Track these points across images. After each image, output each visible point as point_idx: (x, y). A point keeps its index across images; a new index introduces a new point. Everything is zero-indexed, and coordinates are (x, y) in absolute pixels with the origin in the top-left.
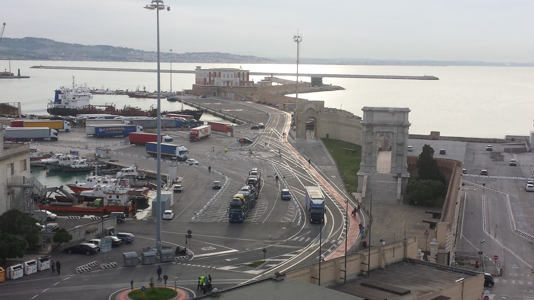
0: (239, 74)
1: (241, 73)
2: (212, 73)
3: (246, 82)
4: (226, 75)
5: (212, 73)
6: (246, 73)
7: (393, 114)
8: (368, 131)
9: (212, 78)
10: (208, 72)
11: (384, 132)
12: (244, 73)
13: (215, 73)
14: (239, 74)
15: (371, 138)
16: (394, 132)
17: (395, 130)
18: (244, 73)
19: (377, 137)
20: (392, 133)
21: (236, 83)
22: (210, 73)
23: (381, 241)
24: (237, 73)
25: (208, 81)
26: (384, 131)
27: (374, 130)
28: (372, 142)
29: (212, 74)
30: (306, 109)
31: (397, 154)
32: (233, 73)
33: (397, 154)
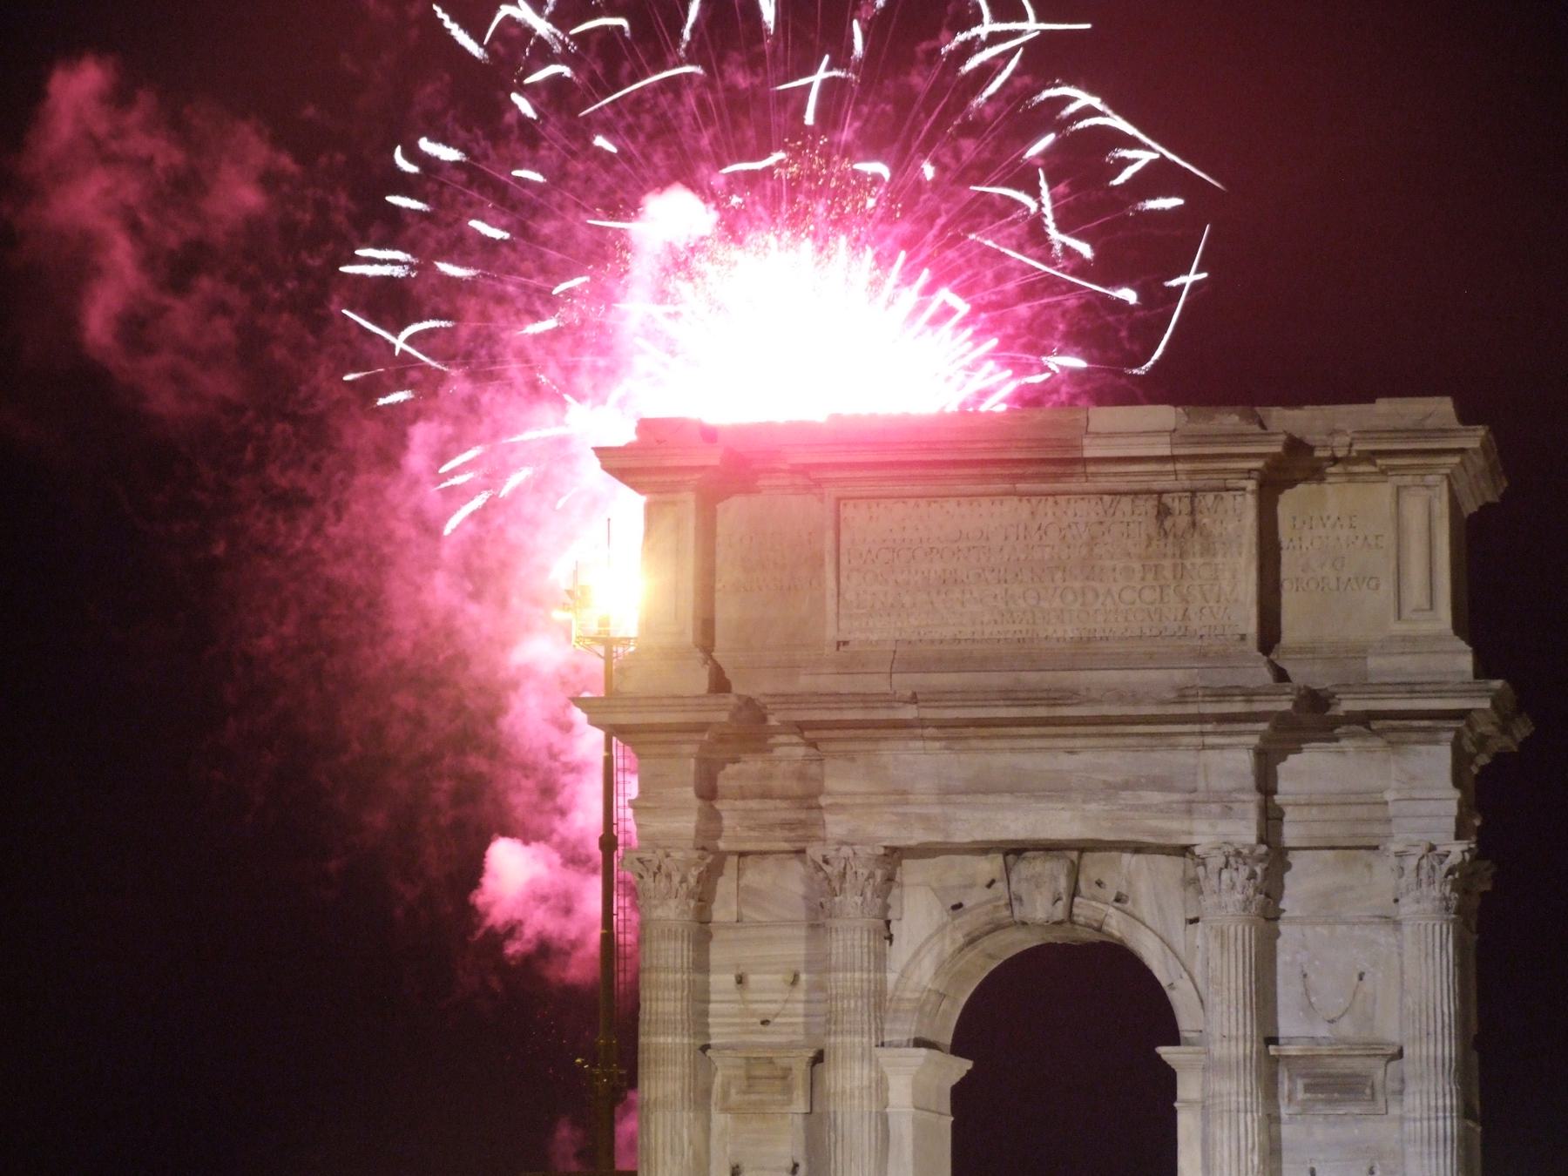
7: (1163, 512)
8: (742, 854)
11: (1015, 851)
15: (795, 981)
16: (1204, 834)
19: (900, 953)
26: (1016, 825)
27: (836, 826)
28: (819, 1058)
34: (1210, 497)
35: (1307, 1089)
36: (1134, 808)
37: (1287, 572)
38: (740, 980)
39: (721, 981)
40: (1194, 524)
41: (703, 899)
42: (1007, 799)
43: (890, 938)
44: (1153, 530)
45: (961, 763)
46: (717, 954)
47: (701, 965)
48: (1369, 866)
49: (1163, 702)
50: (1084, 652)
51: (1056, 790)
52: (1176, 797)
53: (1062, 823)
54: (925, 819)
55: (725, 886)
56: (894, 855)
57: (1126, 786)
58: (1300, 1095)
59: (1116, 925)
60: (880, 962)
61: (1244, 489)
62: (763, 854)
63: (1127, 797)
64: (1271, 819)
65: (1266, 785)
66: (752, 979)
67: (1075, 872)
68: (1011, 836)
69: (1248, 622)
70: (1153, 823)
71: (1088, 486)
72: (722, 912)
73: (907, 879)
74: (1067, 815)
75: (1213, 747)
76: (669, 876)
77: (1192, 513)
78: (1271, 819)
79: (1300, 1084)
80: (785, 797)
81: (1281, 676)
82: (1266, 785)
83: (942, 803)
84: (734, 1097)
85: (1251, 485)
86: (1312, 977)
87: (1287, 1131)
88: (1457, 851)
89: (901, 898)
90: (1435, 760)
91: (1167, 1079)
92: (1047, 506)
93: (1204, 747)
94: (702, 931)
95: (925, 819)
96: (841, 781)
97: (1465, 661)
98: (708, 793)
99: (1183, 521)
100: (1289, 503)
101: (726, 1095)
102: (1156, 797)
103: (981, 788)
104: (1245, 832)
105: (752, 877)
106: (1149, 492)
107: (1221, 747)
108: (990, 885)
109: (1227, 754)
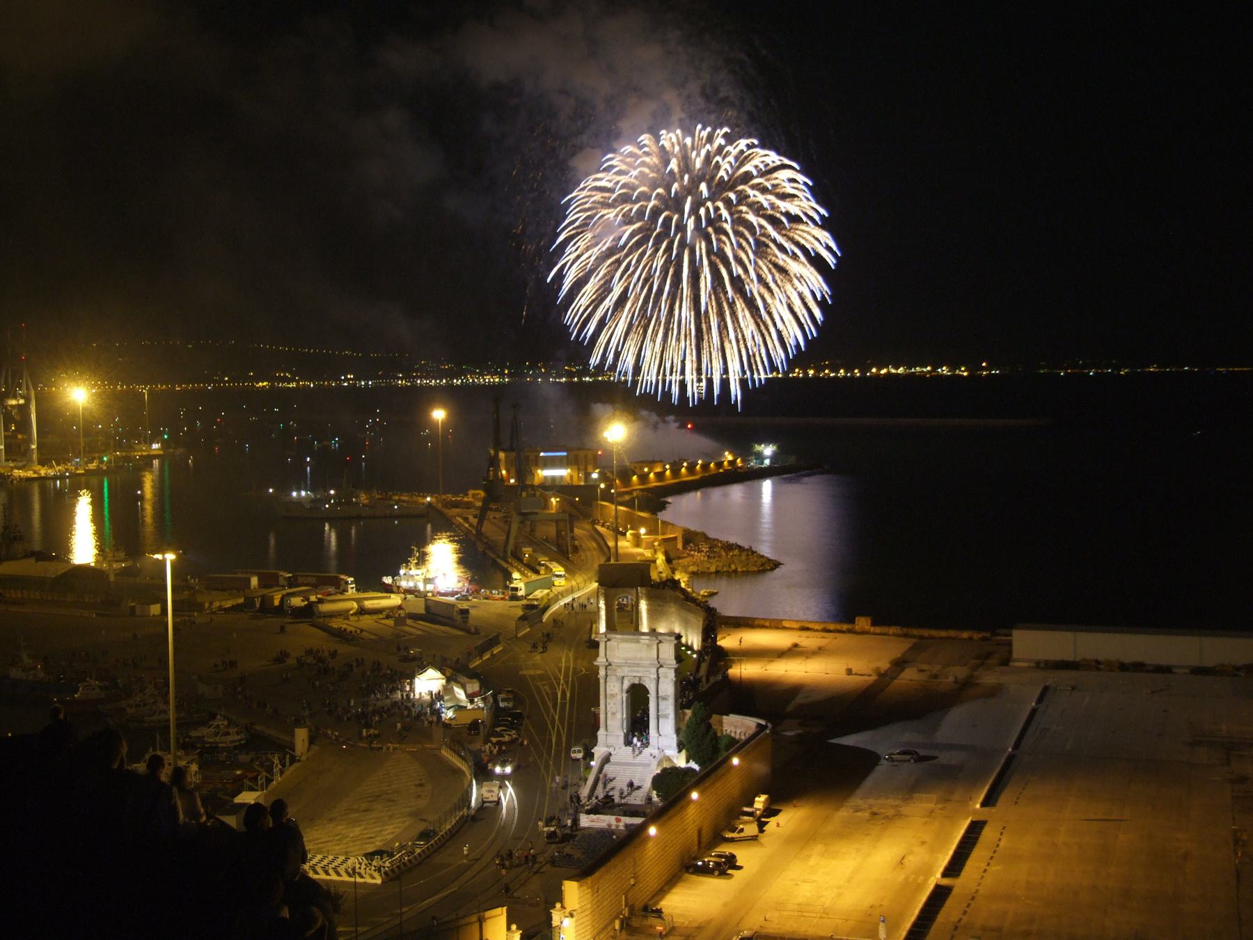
7: (648, 646)
23: (434, 918)
37: (660, 651)
39: (607, 687)
41: (606, 679)
45: (630, 669)
46: (608, 684)
47: (606, 686)
50: (641, 659)
51: (638, 672)
56: (623, 677)
59: (644, 684)
60: (622, 686)
64: (658, 674)
65: (657, 671)
69: (656, 657)
78: (658, 674)
81: (659, 662)
82: (657, 671)
87: (660, 703)
88: (674, 679)
90: (673, 671)
91: (648, 698)
94: (606, 682)
96: (619, 670)
97: (674, 662)
98: (606, 669)
100: (660, 645)
103: (631, 671)
104: (655, 676)
105: (611, 677)
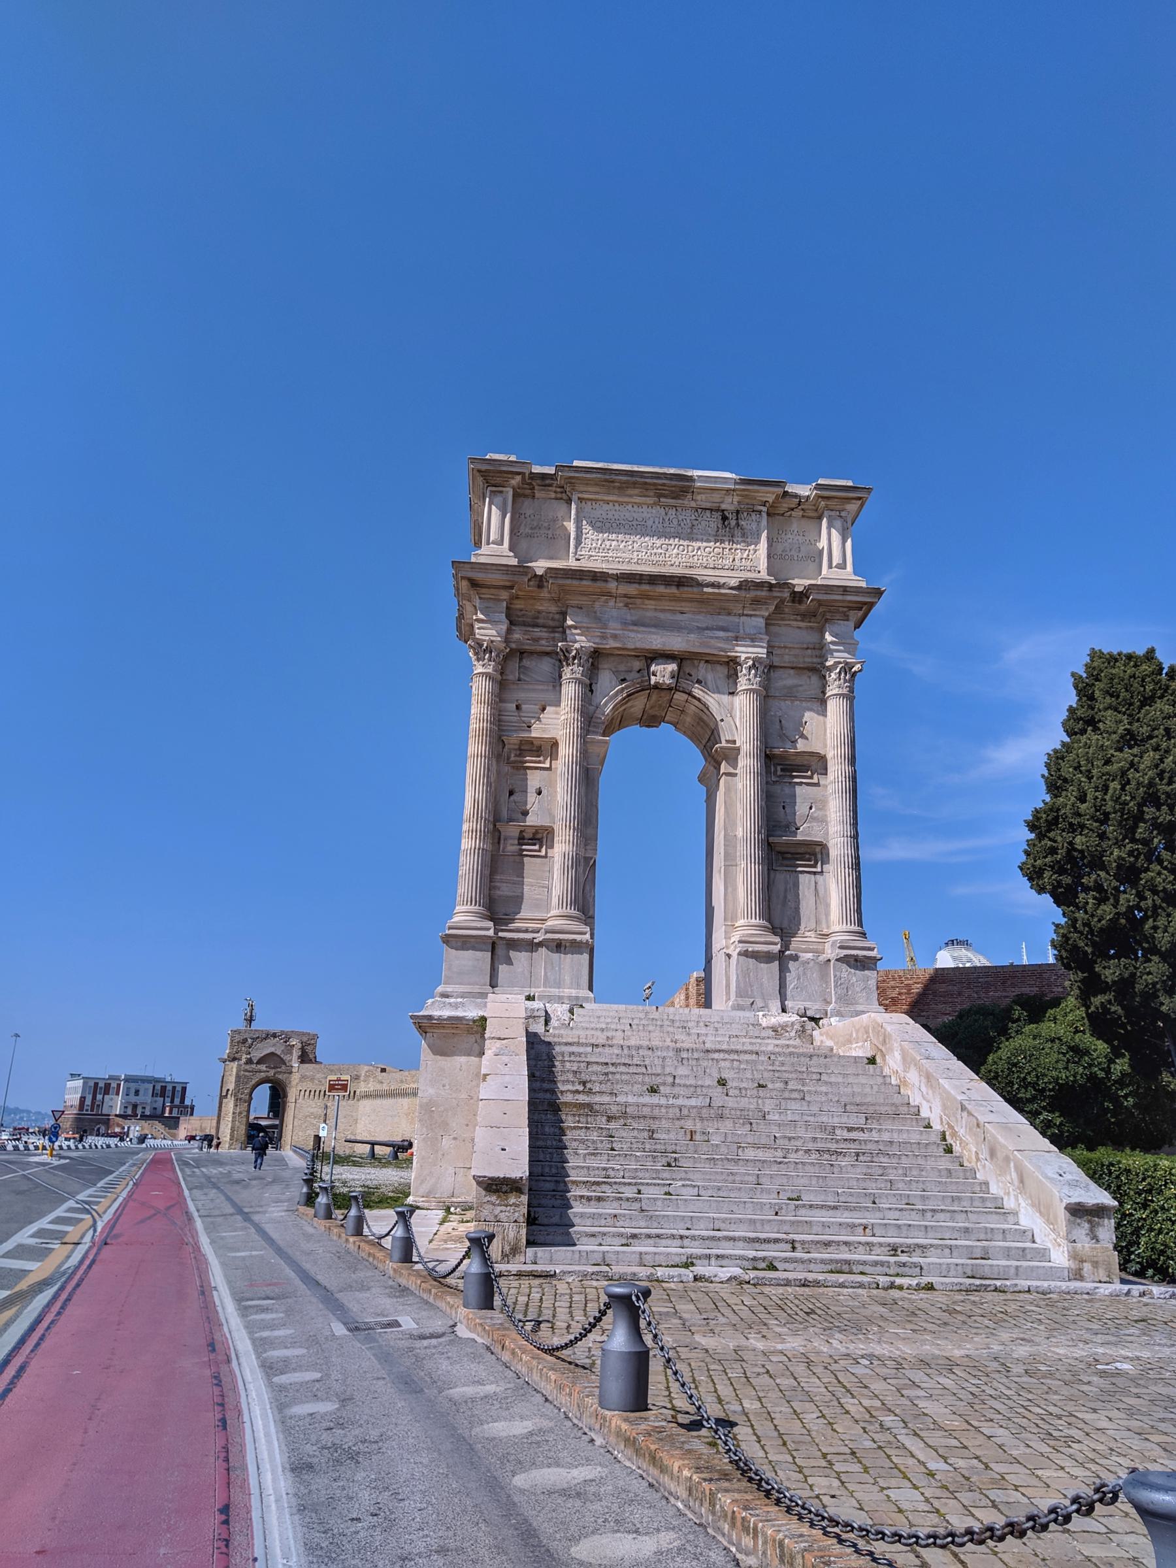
0: (164, 1088)
1: (169, 1088)
2: (101, 1084)
3: (176, 1106)
4: (132, 1091)
5: (101, 1084)
6: (179, 1088)
7: (724, 518)
9: (99, 1097)
10: (92, 1084)
12: (174, 1088)
13: (107, 1087)
14: (164, 1088)
17: (753, 640)
18: (174, 1088)
20: (722, 671)
21: (155, 1109)
22: (96, 1084)
24: (158, 1087)
25: (88, 1102)
26: (657, 641)
29: (101, 1088)
30: (257, 1054)
31: (771, 839)
32: (151, 1086)
33: (769, 844)
34: (745, 514)
35: (782, 770)
36: (712, 638)
38: (518, 707)
40: (738, 525)
42: (653, 630)
43: (591, 691)
44: (720, 526)
48: (810, 677)
49: (731, 588)
52: (730, 634)
53: (676, 642)
54: (615, 637)
55: (514, 665)
57: (707, 628)
58: (779, 773)
61: (760, 512)
62: (532, 653)
63: (710, 633)
66: (524, 707)
67: (680, 667)
68: (654, 647)
70: (719, 645)
71: (693, 504)
72: (512, 676)
73: (600, 666)
74: (679, 639)
75: (747, 615)
76: (491, 652)
77: (737, 519)
79: (779, 768)
80: (544, 627)
83: (623, 630)
84: (513, 758)
85: (764, 509)
86: (783, 722)
89: (597, 674)
92: (672, 512)
93: (743, 615)
95: (615, 637)
99: (733, 523)
101: (508, 758)
102: (721, 634)
105: (526, 662)
106: (717, 510)
107: (751, 616)
108: (638, 672)
109: (753, 618)
